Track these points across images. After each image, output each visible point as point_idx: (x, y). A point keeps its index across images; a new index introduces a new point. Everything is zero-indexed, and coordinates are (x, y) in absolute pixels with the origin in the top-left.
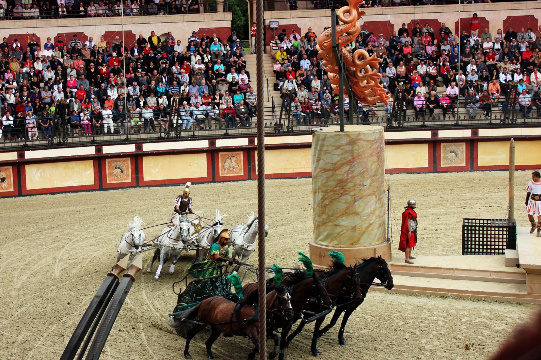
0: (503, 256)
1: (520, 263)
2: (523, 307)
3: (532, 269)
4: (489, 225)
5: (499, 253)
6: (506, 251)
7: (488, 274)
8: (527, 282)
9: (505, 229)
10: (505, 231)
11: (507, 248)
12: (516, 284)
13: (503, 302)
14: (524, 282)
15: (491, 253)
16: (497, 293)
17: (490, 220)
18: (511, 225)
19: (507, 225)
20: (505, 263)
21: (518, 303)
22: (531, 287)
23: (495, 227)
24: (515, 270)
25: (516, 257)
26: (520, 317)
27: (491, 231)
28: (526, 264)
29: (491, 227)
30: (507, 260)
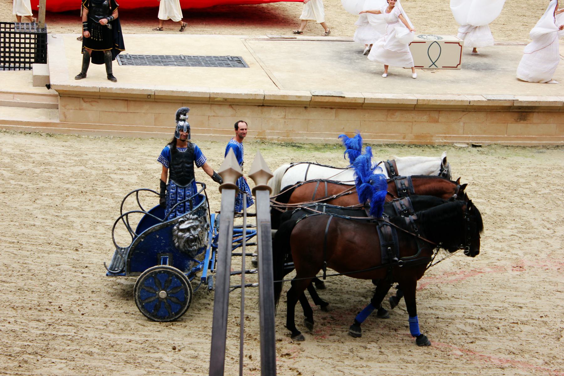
0: (30, 71)
1: (52, 83)
2: (55, 140)
3: (66, 91)
4: (12, 30)
5: (25, 68)
6: (33, 65)
7: (11, 96)
8: (59, 107)
9: (33, 36)
10: (33, 39)
11: (37, 62)
12: (46, 110)
13: (30, 134)
14: (56, 107)
15: (15, 68)
16: (21, 121)
17: (14, 24)
18: (40, 31)
19: (35, 31)
20: (32, 81)
21: (48, 134)
22: (64, 113)
23: (20, 33)
24: (45, 90)
25: (47, 74)
26: (51, 153)
27: (15, 38)
28: (59, 84)
29: (15, 33)
30: (36, 78)
